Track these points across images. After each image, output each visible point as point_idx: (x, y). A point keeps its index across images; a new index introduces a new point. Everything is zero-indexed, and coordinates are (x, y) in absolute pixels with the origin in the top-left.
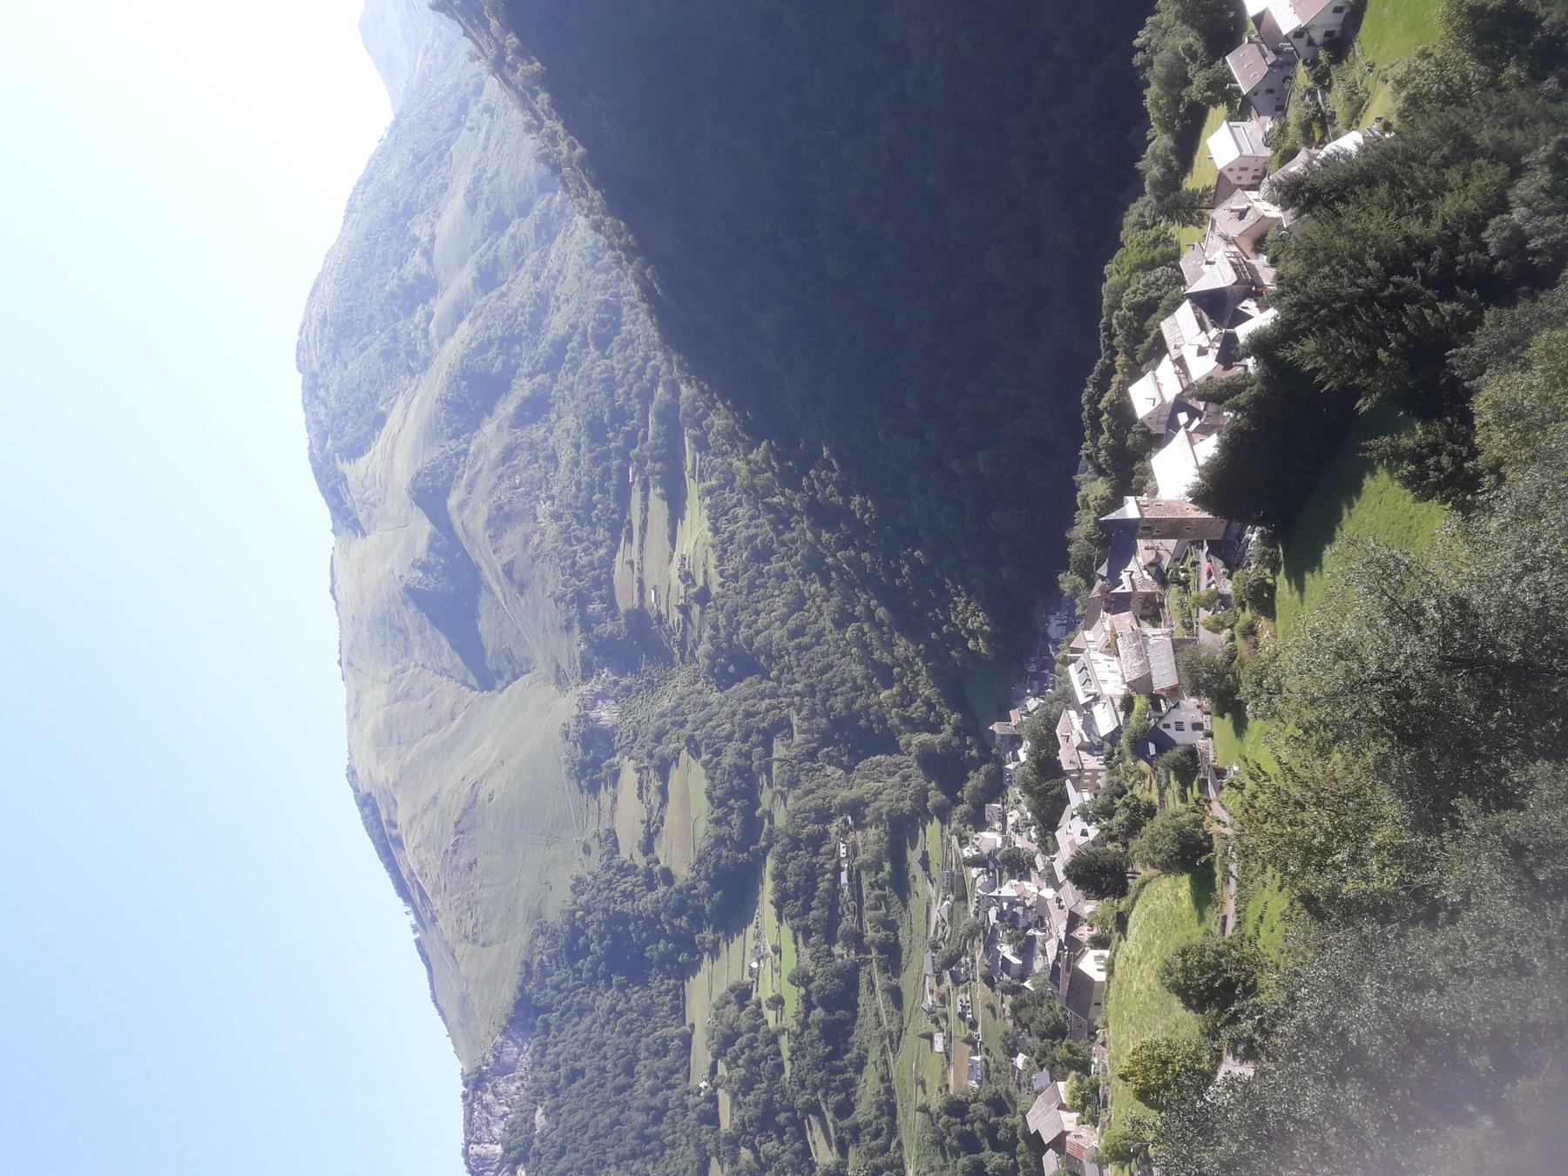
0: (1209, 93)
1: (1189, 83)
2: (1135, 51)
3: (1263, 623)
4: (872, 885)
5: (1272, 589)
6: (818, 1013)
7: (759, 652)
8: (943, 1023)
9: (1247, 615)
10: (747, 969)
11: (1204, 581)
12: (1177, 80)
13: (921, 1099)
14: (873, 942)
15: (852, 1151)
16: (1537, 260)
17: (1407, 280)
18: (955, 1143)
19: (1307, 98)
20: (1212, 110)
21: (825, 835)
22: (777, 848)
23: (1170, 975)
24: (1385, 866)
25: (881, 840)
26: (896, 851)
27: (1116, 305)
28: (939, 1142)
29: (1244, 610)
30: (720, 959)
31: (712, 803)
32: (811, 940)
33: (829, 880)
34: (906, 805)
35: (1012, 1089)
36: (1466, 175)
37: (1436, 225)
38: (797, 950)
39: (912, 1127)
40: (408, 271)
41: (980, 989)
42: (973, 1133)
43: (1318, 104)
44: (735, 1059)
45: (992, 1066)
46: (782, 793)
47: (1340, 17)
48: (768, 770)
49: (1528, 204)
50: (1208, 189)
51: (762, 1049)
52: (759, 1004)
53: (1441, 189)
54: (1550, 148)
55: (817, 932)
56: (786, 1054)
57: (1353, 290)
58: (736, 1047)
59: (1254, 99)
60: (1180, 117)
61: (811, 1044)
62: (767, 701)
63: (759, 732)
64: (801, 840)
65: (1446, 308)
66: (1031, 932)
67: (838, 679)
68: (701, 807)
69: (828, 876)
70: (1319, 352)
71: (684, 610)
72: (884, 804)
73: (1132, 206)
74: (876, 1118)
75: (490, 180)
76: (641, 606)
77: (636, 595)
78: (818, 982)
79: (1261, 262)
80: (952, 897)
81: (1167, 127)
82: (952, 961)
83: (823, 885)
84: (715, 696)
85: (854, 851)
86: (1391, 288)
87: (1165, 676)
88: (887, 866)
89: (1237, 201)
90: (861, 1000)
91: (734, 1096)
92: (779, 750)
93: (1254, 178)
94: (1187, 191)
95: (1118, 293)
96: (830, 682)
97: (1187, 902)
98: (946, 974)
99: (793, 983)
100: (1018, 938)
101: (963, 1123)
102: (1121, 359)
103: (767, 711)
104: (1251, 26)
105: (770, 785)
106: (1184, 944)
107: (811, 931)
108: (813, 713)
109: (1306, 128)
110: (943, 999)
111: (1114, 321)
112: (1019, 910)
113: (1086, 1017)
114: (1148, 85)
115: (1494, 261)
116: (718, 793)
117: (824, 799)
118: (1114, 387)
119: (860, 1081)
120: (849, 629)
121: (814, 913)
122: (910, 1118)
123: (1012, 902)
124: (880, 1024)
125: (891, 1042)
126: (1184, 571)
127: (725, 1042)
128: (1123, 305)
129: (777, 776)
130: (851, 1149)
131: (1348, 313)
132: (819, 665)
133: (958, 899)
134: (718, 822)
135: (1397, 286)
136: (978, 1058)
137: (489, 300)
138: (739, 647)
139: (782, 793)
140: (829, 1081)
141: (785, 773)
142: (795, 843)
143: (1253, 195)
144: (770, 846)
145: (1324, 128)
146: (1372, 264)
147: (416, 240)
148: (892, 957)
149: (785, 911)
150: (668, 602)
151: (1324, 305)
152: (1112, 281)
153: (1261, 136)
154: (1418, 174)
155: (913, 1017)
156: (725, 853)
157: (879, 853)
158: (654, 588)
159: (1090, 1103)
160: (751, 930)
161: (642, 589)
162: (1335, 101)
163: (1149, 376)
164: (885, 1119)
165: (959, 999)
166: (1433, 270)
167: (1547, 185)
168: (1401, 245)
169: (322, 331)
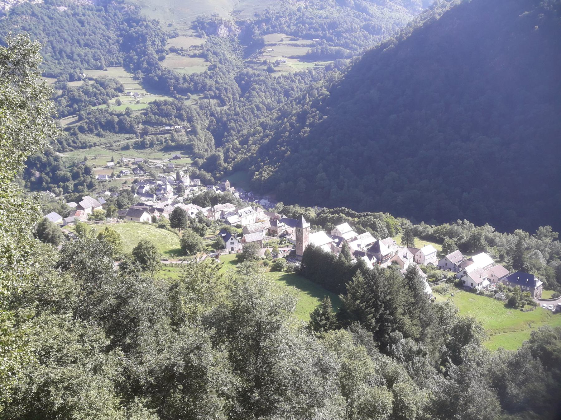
0: (447, 245)
1: (451, 238)
2: (463, 220)
3: (269, 268)
4: (166, 138)
5: (280, 271)
6: (116, 119)
7: (250, 93)
8: (118, 165)
9: (271, 263)
10: (130, 91)
11: (282, 249)
12: (451, 234)
13: (89, 158)
14: (145, 139)
15: (67, 133)
16: (388, 347)
17: (383, 309)
18: (75, 171)
19: (443, 276)
20: (441, 246)
21: (183, 120)
22: (176, 102)
23: (145, 243)
24: (190, 309)
25: (183, 142)
26: (179, 147)
27: (375, 217)
28: (74, 165)
29: (272, 262)
31: (191, 76)
32: (143, 116)
33: (166, 122)
34: (197, 151)
35: (97, 191)
36: (416, 325)
37: (401, 317)
39: (79, 155)
41: (132, 179)
42: (79, 177)
43: (441, 279)
44: (96, 87)
45: (105, 183)
46: (197, 103)
47: (469, 285)
48: (206, 97)
49: (406, 344)
50: (414, 246)
51: (100, 97)
52: (117, 96)
53: (412, 318)
54: (424, 350)
55: (146, 118)
56: (100, 107)
57: (380, 292)
58: (100, 88)
59: (444, 259)
60: (439, 235)
61: (105, 117)
62: (232, 97)
63: (220, 94)
64: (180, 111)
65: (373, 321)
66: (155, 196)
67: (241, 124)
69: (168, 122)
70: (359, 282)
72: (196, 142)
73: (409, 221)
74: (80, 142)
78: (128, 118)
79: (389, 263)
80: (164, 168)
81: (436, 232)
82: (141, 168)
83: (164, 120)
84: (232, 76)
85: (178, 131)
86: (380, 304)
87: (249, 238)
88: (173, 144)
89: (410, 256)
90: (123, 135)
91: (82, 87)
92: (214, 102)
93: (417, 260)
94: (413, 239)
95: (379, 218)
96: (240, 121)
97: (171, 248)
98: (136, 166)
99: (126, 109)
100: (152, 192)
101: (82, 174)
102: (357, 219)
103: (228, 97)
104: (469, 257)
105: (200, 99)
106: (156, 247)
107: (146, 115)
108: (228, 115)
109: (434, 276)
110: (127, 165)
111: (370, 217)
112: (162, 191)
113: (127, 215)
114: (451, 225)
115: (388, 334)
116: (195, 78)
117: (196, 120)
118: (347, 218)
119: (93, 135)
121: (153, 117)
122: (82, 154)
123: (165, 189)
124: (115, 142)
125: (109, 147)
126: (285, 243)
128: (375, 220)
129: (203, 101)
131: (372, 291)
132: (246, 117)
133: (164, 170)
134: (184, 78)
135: (381, 305)
136: (107, 178)
138: (251, 85)
139: (197, 103)
140: (92, 124)
141: (205, 104)
142: (179, 109)
143: (412, 260)
144: (177, 99)
145: (433, 281)
146: (388, 297)
148: (140, 146)
149: (153, 105)
151: (375, 283)
152: (383, 215)
153: (432, 262)
154: (417, 311)
155: (120, 155)
156: (173, 81)
157: (178, 141)
159: (96, 218)
160: (144, 92)
162: (442, 285)
163: (351, 229)
164: (80, 145)
165: (128, 171)
166: (386, 316)
167: (412, 349)
168: (394, 306)
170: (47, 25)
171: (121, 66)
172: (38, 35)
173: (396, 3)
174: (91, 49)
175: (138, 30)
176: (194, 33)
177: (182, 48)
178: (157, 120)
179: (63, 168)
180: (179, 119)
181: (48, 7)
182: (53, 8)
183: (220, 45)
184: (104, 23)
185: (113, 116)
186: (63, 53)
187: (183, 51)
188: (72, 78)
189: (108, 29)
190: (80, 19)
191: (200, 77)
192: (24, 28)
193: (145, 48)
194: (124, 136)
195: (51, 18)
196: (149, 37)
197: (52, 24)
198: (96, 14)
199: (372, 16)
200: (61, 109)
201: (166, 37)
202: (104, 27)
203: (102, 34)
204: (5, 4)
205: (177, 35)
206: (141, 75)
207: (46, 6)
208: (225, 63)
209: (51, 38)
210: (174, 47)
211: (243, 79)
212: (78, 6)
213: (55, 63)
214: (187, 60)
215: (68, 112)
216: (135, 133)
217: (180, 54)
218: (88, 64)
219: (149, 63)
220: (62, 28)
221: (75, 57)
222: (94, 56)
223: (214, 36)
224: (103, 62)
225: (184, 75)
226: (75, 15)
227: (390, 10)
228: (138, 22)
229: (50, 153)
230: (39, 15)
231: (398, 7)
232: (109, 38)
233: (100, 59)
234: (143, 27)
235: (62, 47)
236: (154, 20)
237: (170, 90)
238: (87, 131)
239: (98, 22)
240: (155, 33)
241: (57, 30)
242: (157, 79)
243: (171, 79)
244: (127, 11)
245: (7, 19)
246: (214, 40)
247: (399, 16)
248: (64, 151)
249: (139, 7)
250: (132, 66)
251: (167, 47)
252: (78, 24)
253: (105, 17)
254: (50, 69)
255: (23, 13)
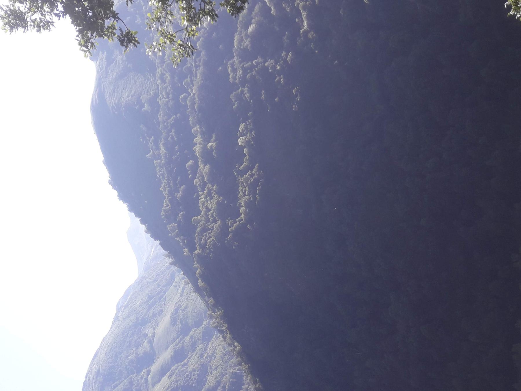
40: (141, 351)
75: (183, 310)
137: (178, 367)
147: (146, 335)
169: (96, 378)
173: (205, 350)
199: (219, 383)
227: (213, 358)
231: (209, 347)
247: (220, 347)
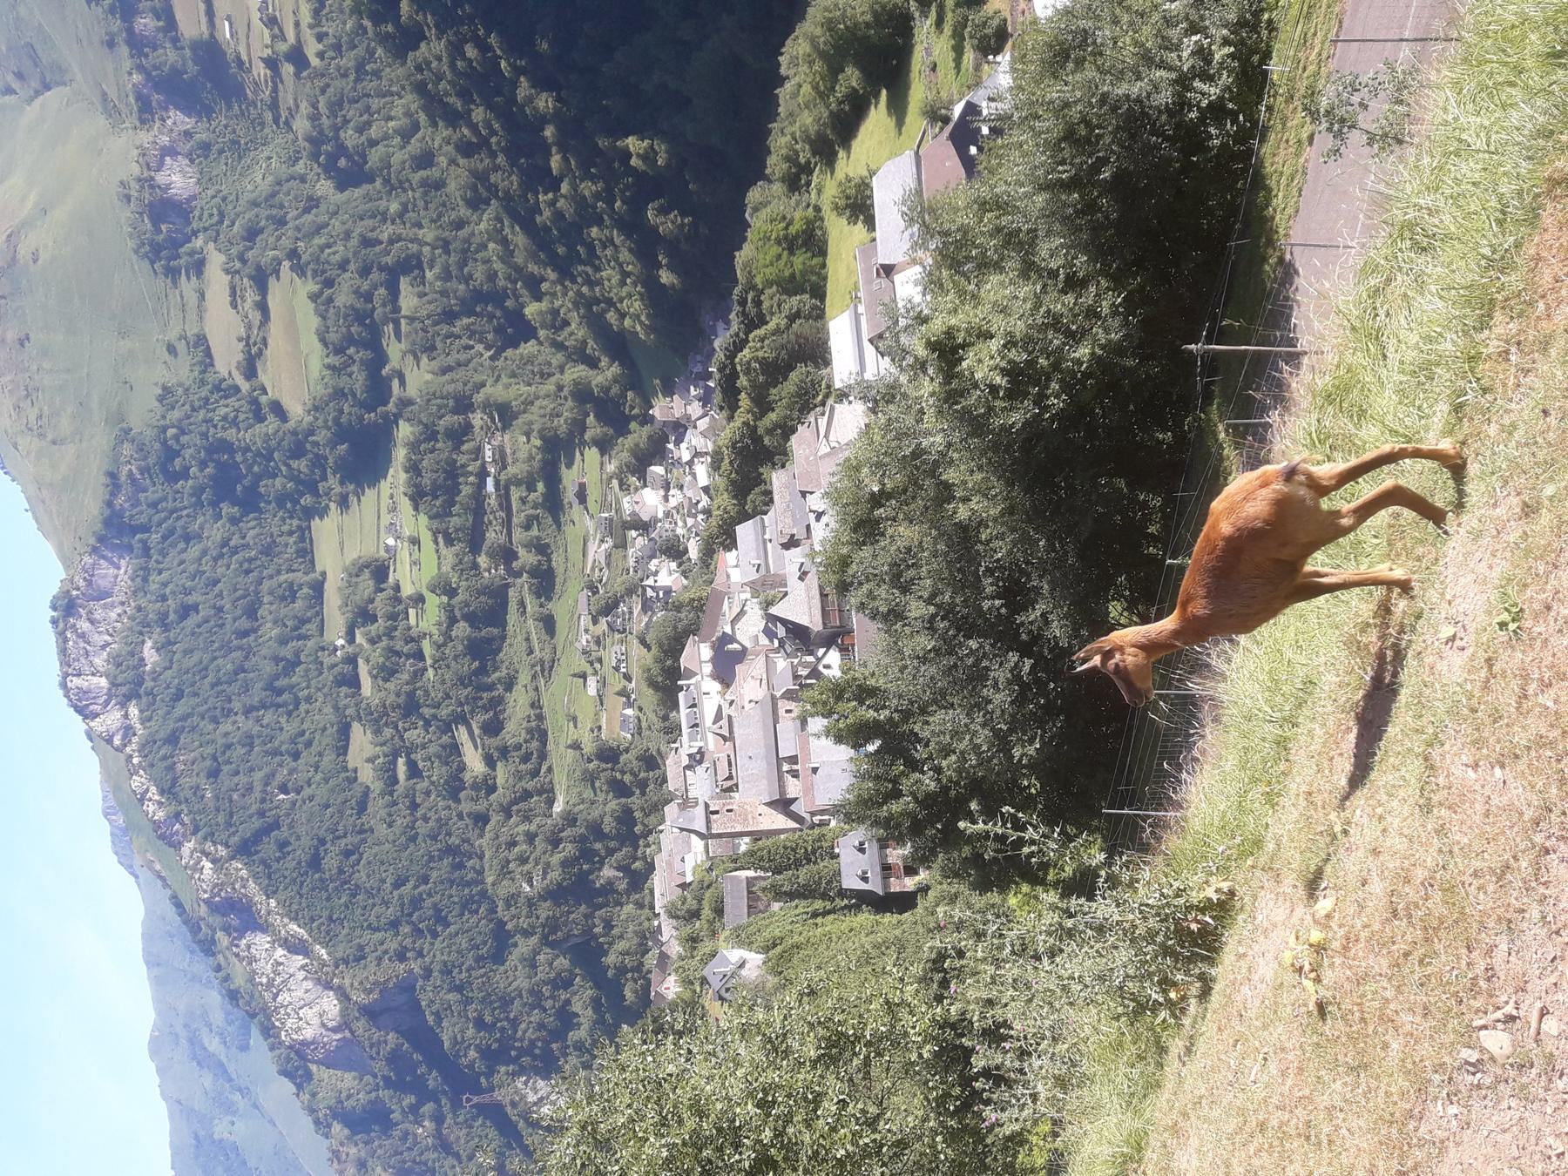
6: (462, 629)
10: (382, 546)
13: (572, 734)
21: (468, 427)
25: (531, 458)
26: (551, 474)
30: (350, 512)
38: (437, 551)
39: (563, 767)
52: (397, 588)
55: (459, 540)
61: (456, 658)
64: (438, 432)
68: (316, 358)
69: (471, 479)
71: (271, 63)
74: (526, 741)
76: (212, 36)
77: (204, 20)
83: (466, 490)
84: (324, 187)
88: (540, 486)
91: (375, 677)
92: (408, 300)
96: (467, 241)
99: (433, 592)
103: (391, 242)
108: (446, 275)
110: (598, 642)
116: (333, 337)
117: (465, 384)
120: (485, 217)
121: (455, 521)
124: (531, 652)
125: (543, 671)
127: (365, 615)
129: (407, 336)
130: (499, 764)
140: (475, 699)
142: (430, 434)
148: (545, 582)
150: (248, 45)
156: (346, 408)
158: (229, 18)
161: (210, 13)
164: (535, 744)
170: (201, 709)
171: (309, 528)
172: (230, 740)
174: (261, 604)
175: (192, 457)
176: (189, 279)
177: (240, 340)
178: (466, 509)
179: (595, 814)
180: (463, 443)
181: (147, 694)
182: (149, 684)
183: (224, 199)
184: (182, 545)
185: (453, 634)
186: (277, 684)
187: (248, 337)
188: (354, 682)
189: (199, 537)
190: (175, 612)
191: (330, 323)
192: (214, 774)
193: (247, 449)
194: (512, 616)
195: (179, 696)
196: (212, 430)
197: (196, 695)
198: (158, 562)
200: (433, 749)
201: (210, 377)
202: (194, 551)
203: (215, 559)
204: (150, 800)
205: (201, 341)
206: (333, 482)
207: (144, 699)
208: (282, 207)
209: (236, 705)
210: (239, 363)
211: (332, 159)
212: (139, 609)
213: (307, 712)
214: (276, 329)
215: (444, 732)
216: (507, 586)
217: (260, 350)
218: (308, 621)
219: (298, 451)
220: (206, 669)
221: (287, 652)
222: (283, 598)
223: (197, 213)
224: (299, 577)
225: (329, 367)
226: (166, 627)
228: (170, 454)
229: (553, 832)
230: (171, 725)
232: (225, 543)
233: (291, 584)
234: (184, 439)
235: (259, 685)
236: (161, 399)
237: (376, 424)
238: (495, 713)
239: (182, 562)
240: (200, 408)
241: (213, 686)
242: (344, 447)
243: (341, 411)
244: (142, 471)
245: (190, 812)
246: (211, 215)
248: (552, 790)
249: (121, 429)
250: (307, 500)
251: (245, 386)
252: (191, 622)
253: (165, 538)
254: (324, 729)
255: (171, 768)
